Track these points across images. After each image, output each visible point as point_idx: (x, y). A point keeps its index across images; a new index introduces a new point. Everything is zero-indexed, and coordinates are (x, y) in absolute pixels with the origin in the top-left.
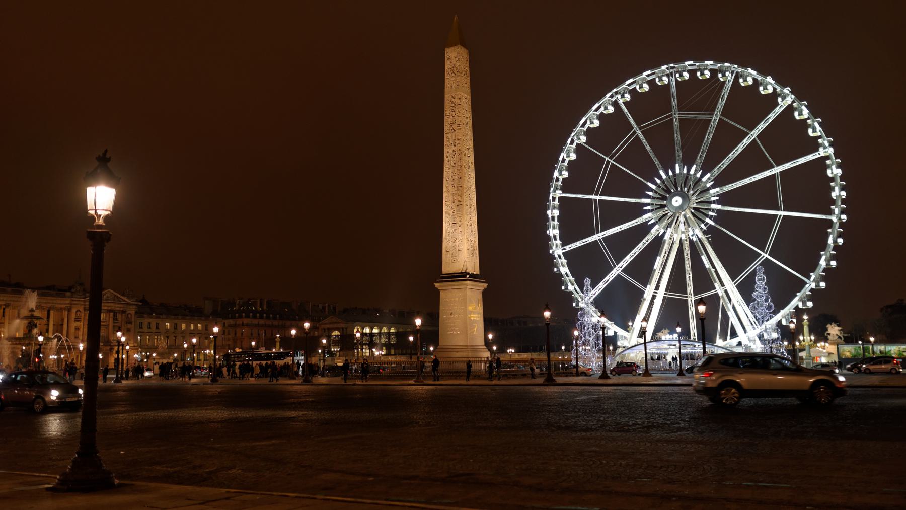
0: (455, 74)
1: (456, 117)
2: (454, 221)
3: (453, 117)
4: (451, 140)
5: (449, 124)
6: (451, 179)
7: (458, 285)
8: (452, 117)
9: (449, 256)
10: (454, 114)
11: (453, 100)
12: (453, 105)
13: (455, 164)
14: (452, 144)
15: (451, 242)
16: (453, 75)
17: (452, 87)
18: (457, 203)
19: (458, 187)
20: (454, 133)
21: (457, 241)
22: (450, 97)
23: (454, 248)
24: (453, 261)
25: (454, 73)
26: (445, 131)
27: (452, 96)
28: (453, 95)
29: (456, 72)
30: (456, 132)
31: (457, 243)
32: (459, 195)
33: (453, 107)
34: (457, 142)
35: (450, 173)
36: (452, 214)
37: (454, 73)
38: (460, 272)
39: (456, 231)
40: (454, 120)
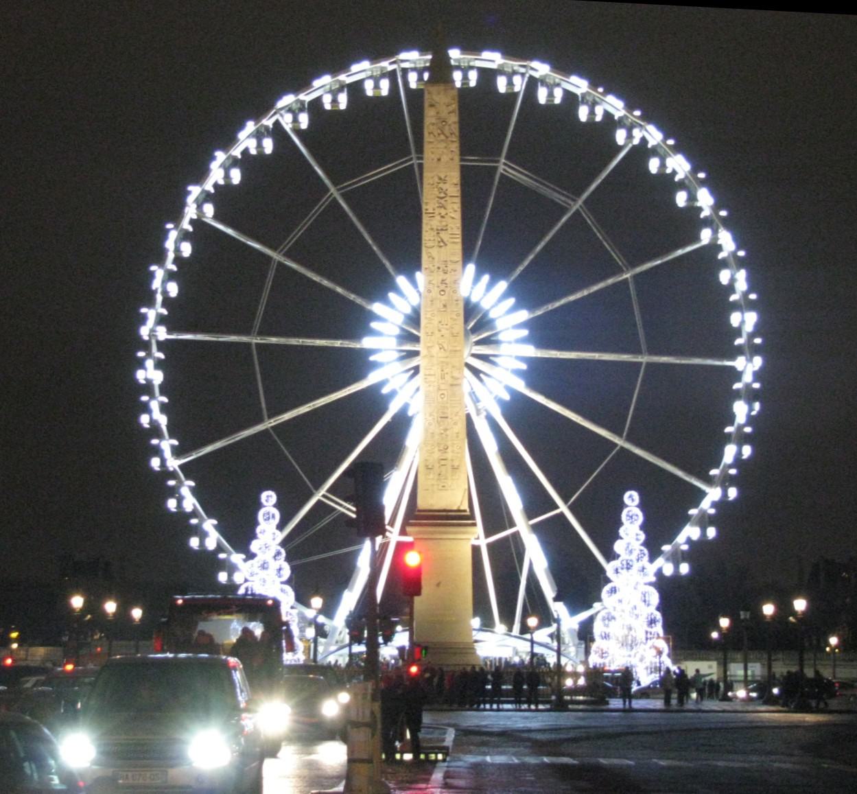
0: (447, 137)
1: (448, 219)
2: (443, 413)
3: (443, 217)
4: (436, 260)
5: (432, 229)
6: (438, 334)
8: (438, 218)
9: (431, 476)
10: (443, 212)
11: (441, 185)
12: (442, 195)
13: (445, 306)
14: (439, 268)
15: (436, 449)
16: (442, 137)
17: (439, 160)
18: (450, 381)
19: (451, 351)
21: (449, 450)
22: (436, 179)
23: (443, 462)
24: (440, 487)
25: (443, 133)
27: (440, 179)
28: (443, 177)
29: (448, 134)
30: (448, 247)
31: (449, 455)
32: (453, 367)
34: (450, 267)
35: (435, 322)
36: (441, 400)
37: (443, 133)
38: (455, 508)
39: (448, 432)
40: (444, 223)
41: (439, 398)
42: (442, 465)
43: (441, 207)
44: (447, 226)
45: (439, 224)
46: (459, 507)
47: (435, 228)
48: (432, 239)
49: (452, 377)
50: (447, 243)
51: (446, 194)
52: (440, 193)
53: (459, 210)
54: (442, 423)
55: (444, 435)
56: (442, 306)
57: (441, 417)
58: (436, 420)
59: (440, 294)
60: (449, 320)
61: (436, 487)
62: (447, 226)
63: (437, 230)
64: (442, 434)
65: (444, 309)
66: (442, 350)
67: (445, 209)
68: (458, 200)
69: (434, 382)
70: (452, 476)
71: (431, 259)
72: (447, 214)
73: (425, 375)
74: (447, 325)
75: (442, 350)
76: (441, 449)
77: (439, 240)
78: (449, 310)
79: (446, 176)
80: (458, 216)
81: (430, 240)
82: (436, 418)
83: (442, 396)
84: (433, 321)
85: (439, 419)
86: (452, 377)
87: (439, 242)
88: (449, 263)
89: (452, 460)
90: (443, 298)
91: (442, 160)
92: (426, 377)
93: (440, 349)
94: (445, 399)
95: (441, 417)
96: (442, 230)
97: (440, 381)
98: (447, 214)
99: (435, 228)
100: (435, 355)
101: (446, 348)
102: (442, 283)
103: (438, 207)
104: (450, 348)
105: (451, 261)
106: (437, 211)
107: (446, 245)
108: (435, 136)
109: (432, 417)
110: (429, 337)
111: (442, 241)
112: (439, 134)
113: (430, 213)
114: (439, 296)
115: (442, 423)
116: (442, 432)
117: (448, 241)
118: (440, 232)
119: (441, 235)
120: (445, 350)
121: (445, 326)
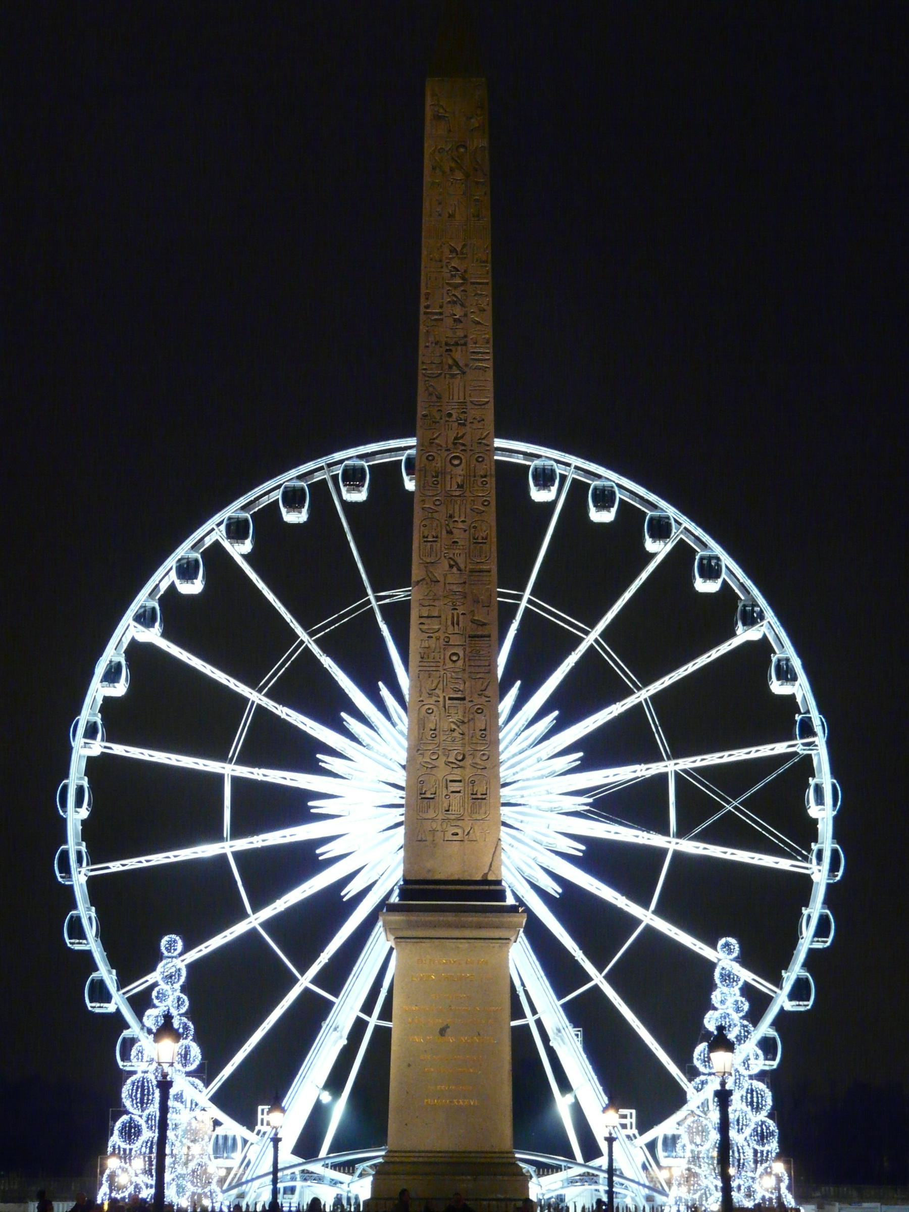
7: (480, 926)
8: (449, 322)
9: (431, 814)
10: (458, 312)
15: (441, 762)
19: (472, 571)
20: (457, 381)
22: (446, 250)
26: (421, 366)
27: (453, 250)
33: (456, 286)
36: (449, 665)
40: (460, 334)
41: (447, 660)
42: (453, 792)
43: (455, 302)
44: (466, 336)
45: (450, 334)
46: (486, 874)
47: (443, 340)
48: (437, 361)
49: (473, 621)
50: (466, 369)
51: (463, 278)
52: (453, 276)
53: (489, 309)
54: (452, 711)
55: (456, 734)
56: (455, 487)
57: (450, 699)
58: (441, 703)
59: (452, 465)
60: (468, 510)
61: (440, 834)
62: (466, 336)
63: (447, 344)
64: (454, 730)
65: (457, 494)
66: (455, 570)
67: (463, 305)
68: (487, 291)
69: (439, 629)
70: (472, 812)
71: (434, 399)
72: (466, 315)
73: (421, 617)
74: (463, 522)
75: (455, 569)
76: (452, 759)
77: (450, 362)
78: (468, 494)
79: (464, 246)
80: (487, 320)
81: (432, 363)
82: (441, 699)
83: (455, 658)
84: (435, 515)
85: (448, 702)
86: (473, 621)
87: (450, 367)
88: (469, 406)
89: (473, 782)
90: (459, 471)
91: (458, 217)
92: (422, 620)
93: (451, 566)
94: (460, 663)
95: (450, 699)
96: (457, 344)
97: (450, 630)
98: (466, 315)
99: (443, 340)
100: (441, 579)
101: (462, 566)
102: (455, 444)
103: (449, 302)
104: (470, 566)
105: (471, 402)
106: (448, 310)
107: (464, 373)
108: (444, 172)
109: (435, 698)
110: (429, 544)
111: (456, 364)
112: (452, 170)
113: (436, 314)
114: (449, 468)
115: (452, 711)
116: (454, 726)
117: (466, 365)
118: (453, 348)
119: (453, 354)
120: (459, 569)
121: (461, 525)
